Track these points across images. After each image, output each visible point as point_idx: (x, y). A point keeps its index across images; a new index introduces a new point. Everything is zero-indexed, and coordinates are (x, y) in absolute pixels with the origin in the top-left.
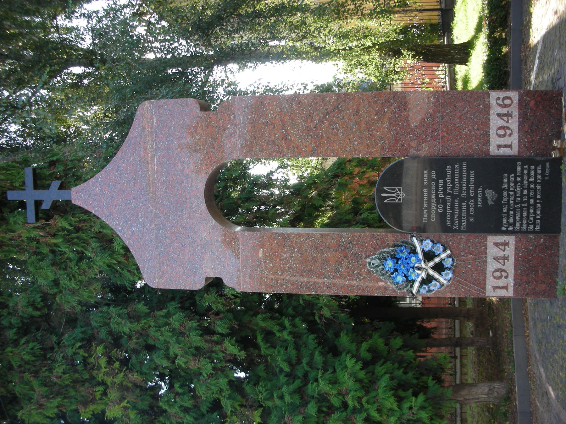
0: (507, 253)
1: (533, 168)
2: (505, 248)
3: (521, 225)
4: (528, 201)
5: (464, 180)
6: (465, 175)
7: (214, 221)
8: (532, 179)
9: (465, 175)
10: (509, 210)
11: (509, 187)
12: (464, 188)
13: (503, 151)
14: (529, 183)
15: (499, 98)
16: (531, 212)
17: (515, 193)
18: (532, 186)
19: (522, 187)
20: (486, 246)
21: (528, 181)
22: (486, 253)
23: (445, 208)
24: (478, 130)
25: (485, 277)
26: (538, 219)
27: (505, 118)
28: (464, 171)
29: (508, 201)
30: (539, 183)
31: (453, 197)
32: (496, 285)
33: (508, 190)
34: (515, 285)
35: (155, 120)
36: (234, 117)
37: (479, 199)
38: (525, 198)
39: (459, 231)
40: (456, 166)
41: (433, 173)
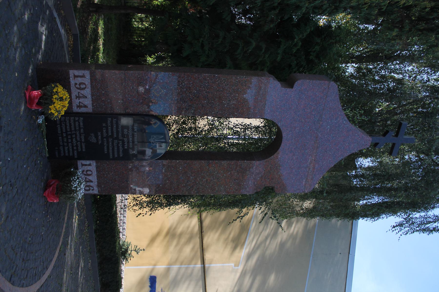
0: (77, 101)
1: (67, 154)
2: (79, 94)
3: (70, 121)
5: (111, 148)
6: (111, 151)
8: (66, 148)
9: (111, 151)
11: (81, 144)
12: (111, 143)
13: (88, 162)
14: (68, 146)
15: (93, 190)
16: (64, 128)
17: (76, 140)
18: (65, 144)
19: (72, 144)
20: (93, 106)
21: (69, 147)
22: (92, 101)
24: (104, 174)
25: (91, 84)
26: (59, 124)
27: (87, 180)
29: (80, 135)
30: (61, 146)
31: (117, 138)
32: (83, 78)
34: (69, 78)
35: (304, 183)
36: (254, 183)
37: (100, 137)
38: (69, 137)
40: (116, 156)
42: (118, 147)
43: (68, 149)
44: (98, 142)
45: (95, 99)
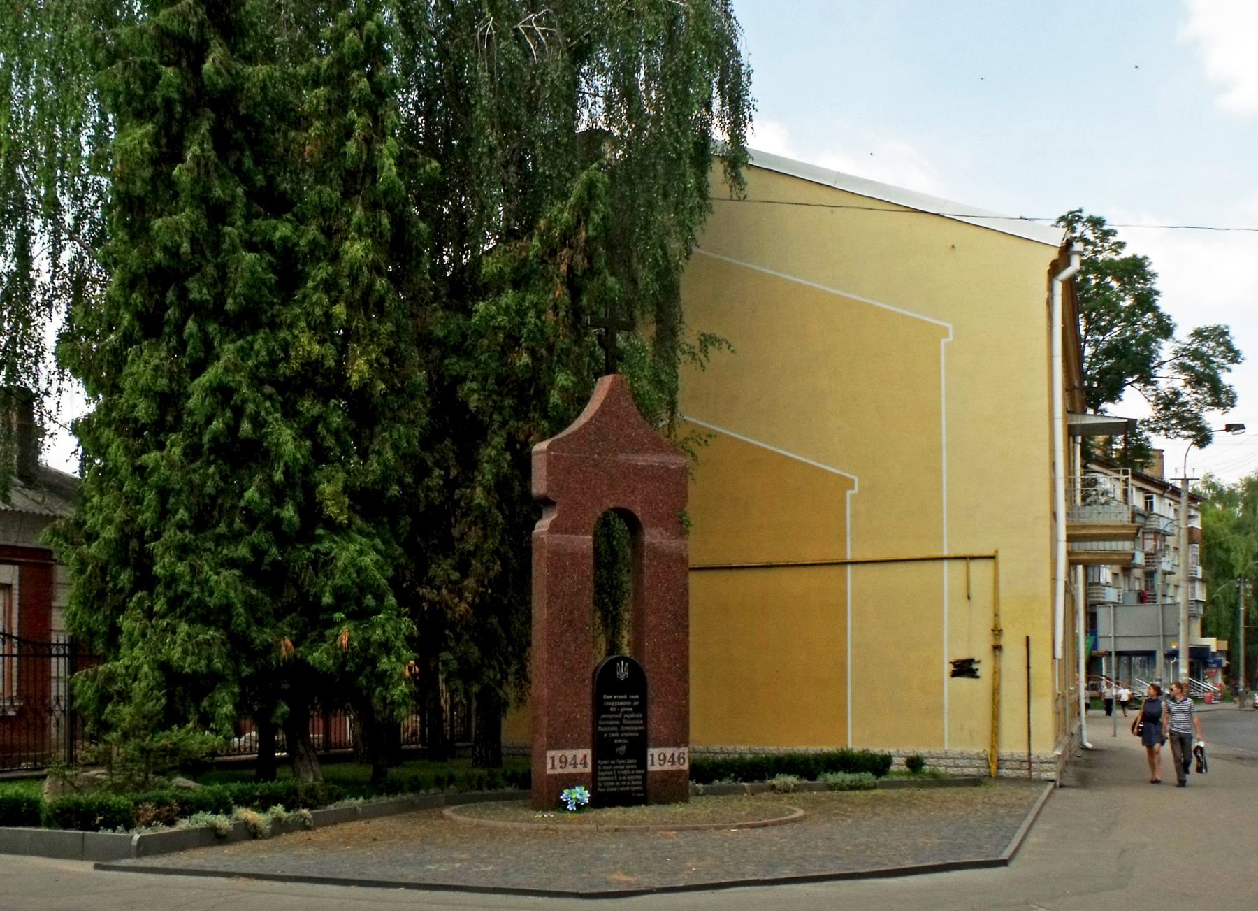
13: (649, 758)
31: (620, 720)
41: (636, 703)
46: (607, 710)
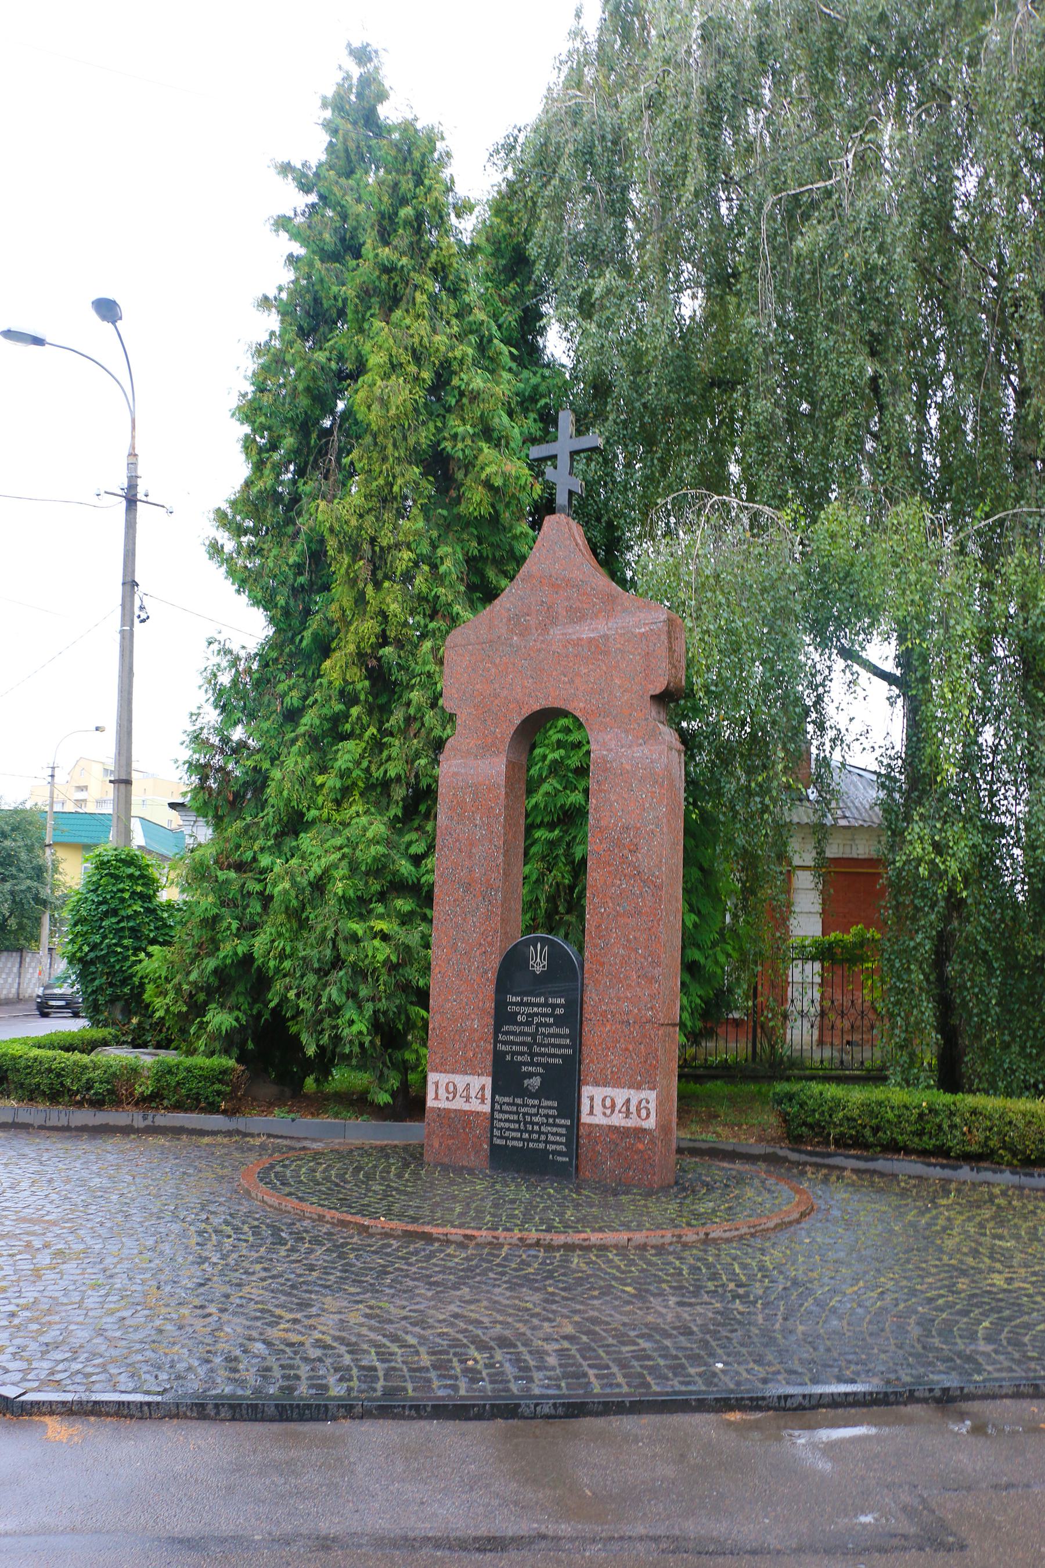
3: (500, 1120)
4: (526, 1131)
5: (553, 1051)
7: (518, 722)
8: (551, 1138)
9: (557, 1051)
10: (518, 1105)
13: (585, 1103)
14: (546, 1134)
17: (536, 1115)
18: (543, 1138)
20: (482, 1074)
23: (521, 1024)
27: (624, 1109)
28: (562, 1051)
29: (527, 1106)
31: (534, 1036)
33: (539, 1107)
39: (496, 1041)
42: (551, 1035)
43: (553, 1134)
44: (539, 1074)
45: (468, 1068)
46: (512, 1019)
